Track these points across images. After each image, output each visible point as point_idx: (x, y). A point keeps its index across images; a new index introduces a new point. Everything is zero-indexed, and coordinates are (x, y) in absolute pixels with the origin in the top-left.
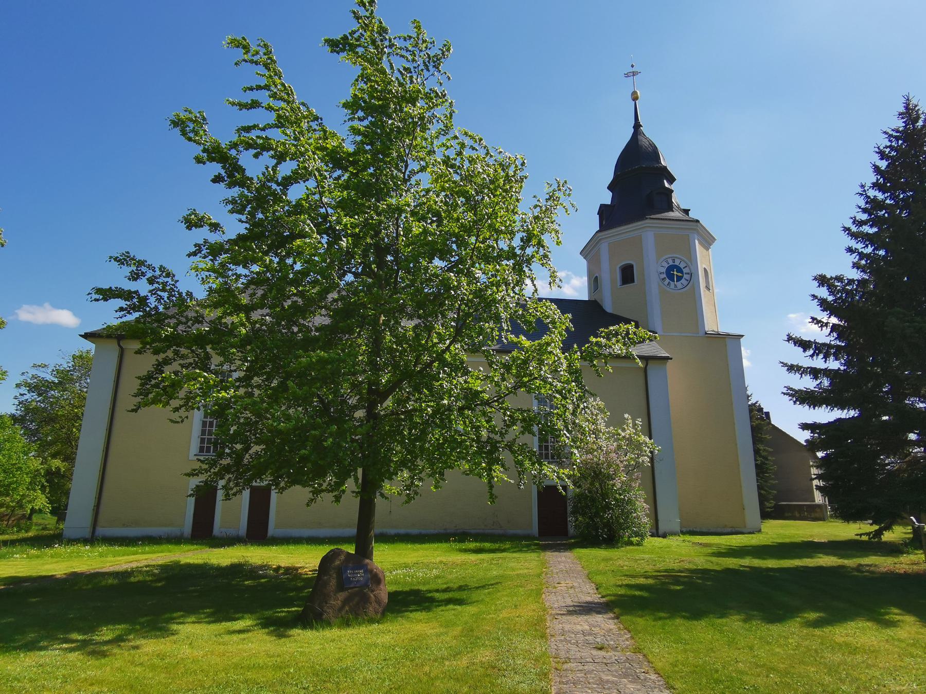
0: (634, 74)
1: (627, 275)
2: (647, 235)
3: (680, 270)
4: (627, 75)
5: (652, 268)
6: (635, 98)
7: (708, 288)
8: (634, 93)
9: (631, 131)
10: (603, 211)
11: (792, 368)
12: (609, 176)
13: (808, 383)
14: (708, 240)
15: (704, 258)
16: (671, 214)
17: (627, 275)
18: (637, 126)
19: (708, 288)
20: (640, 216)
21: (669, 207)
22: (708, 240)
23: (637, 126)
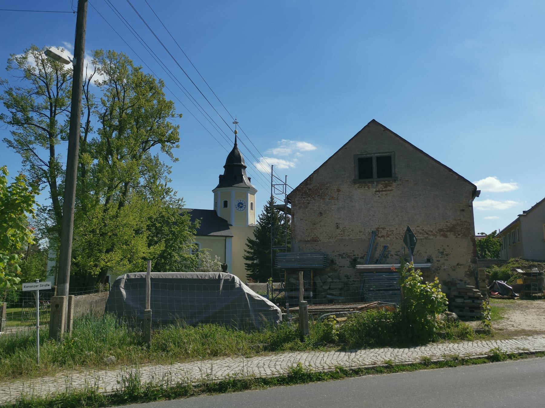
0: (236, 123)
1: (226, 204)
2: (233, 191)
3: (242, 204)
4: (234, 123)
5: (233, 204)
6: (236, 133)
7: (252, 209)
8: (235, 131)
9: (233, 146)
10: (221, 177)
11: (245, 251)
12: (224, 164)
13: (248, 255)
14: (254, 191)
15: (251, 198)
16: (241, 185)
17: (226, 204)
18: (236, 145)
19: (252, 209)
20: (230, 185)
21: (242, 181)
22: (254, 191)
23: (236, 145)
